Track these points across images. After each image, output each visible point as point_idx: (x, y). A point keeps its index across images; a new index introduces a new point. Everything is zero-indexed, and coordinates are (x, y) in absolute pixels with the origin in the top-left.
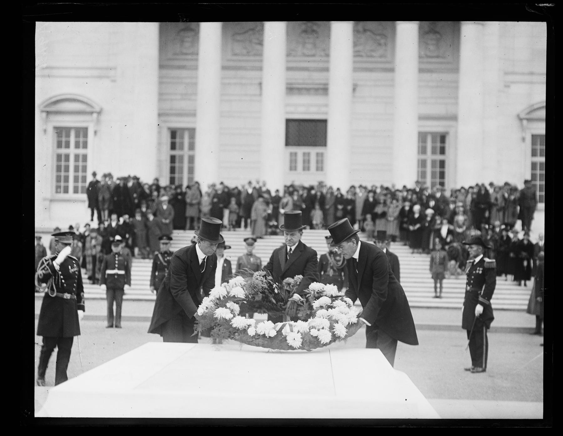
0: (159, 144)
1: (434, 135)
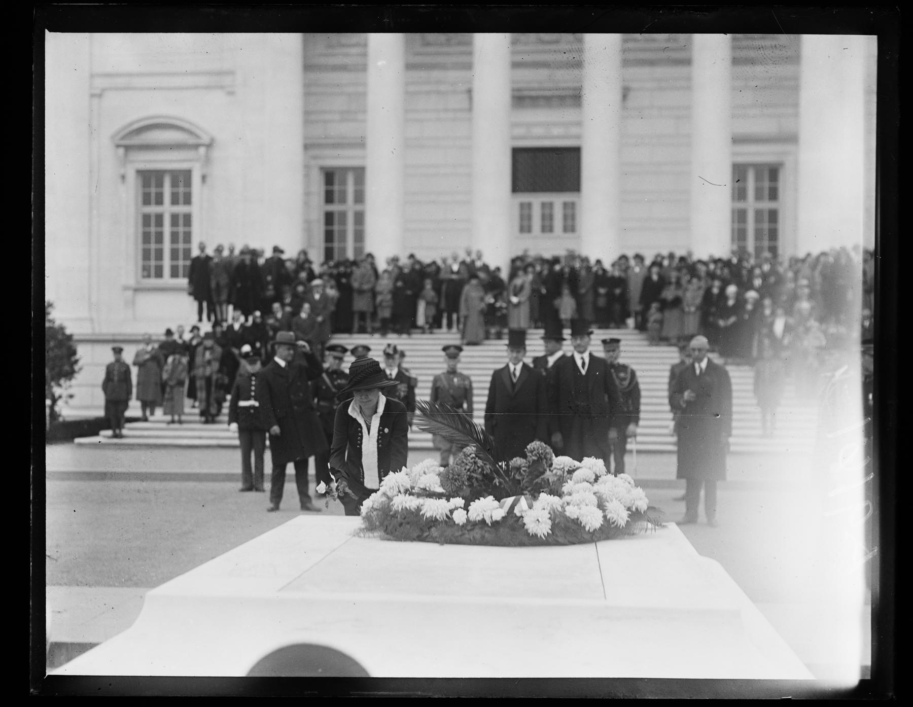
0: (307, 194)
1: (759, 168)
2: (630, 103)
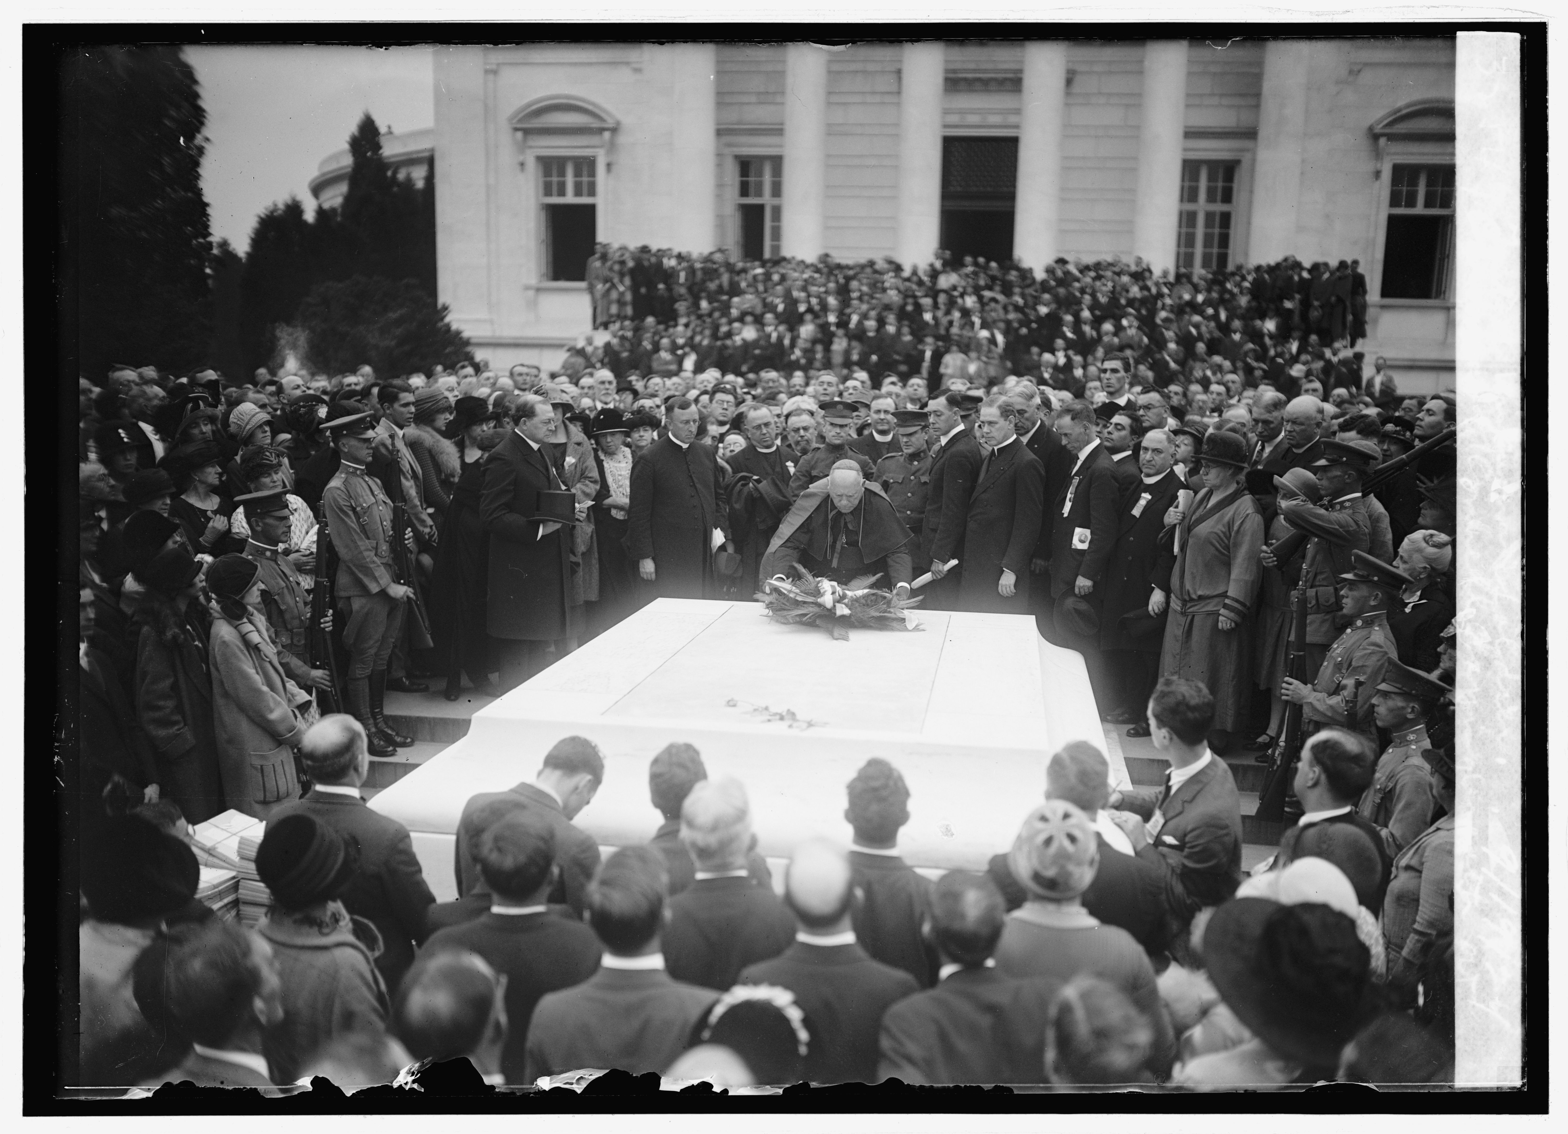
0: (720, 185)
1: (1213, 165)
2: (1076, 88)
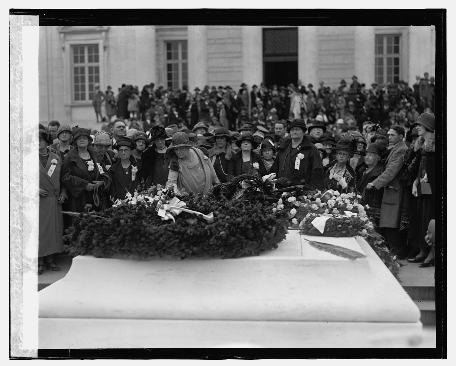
0: (157, 55)
1: (388, 36)
